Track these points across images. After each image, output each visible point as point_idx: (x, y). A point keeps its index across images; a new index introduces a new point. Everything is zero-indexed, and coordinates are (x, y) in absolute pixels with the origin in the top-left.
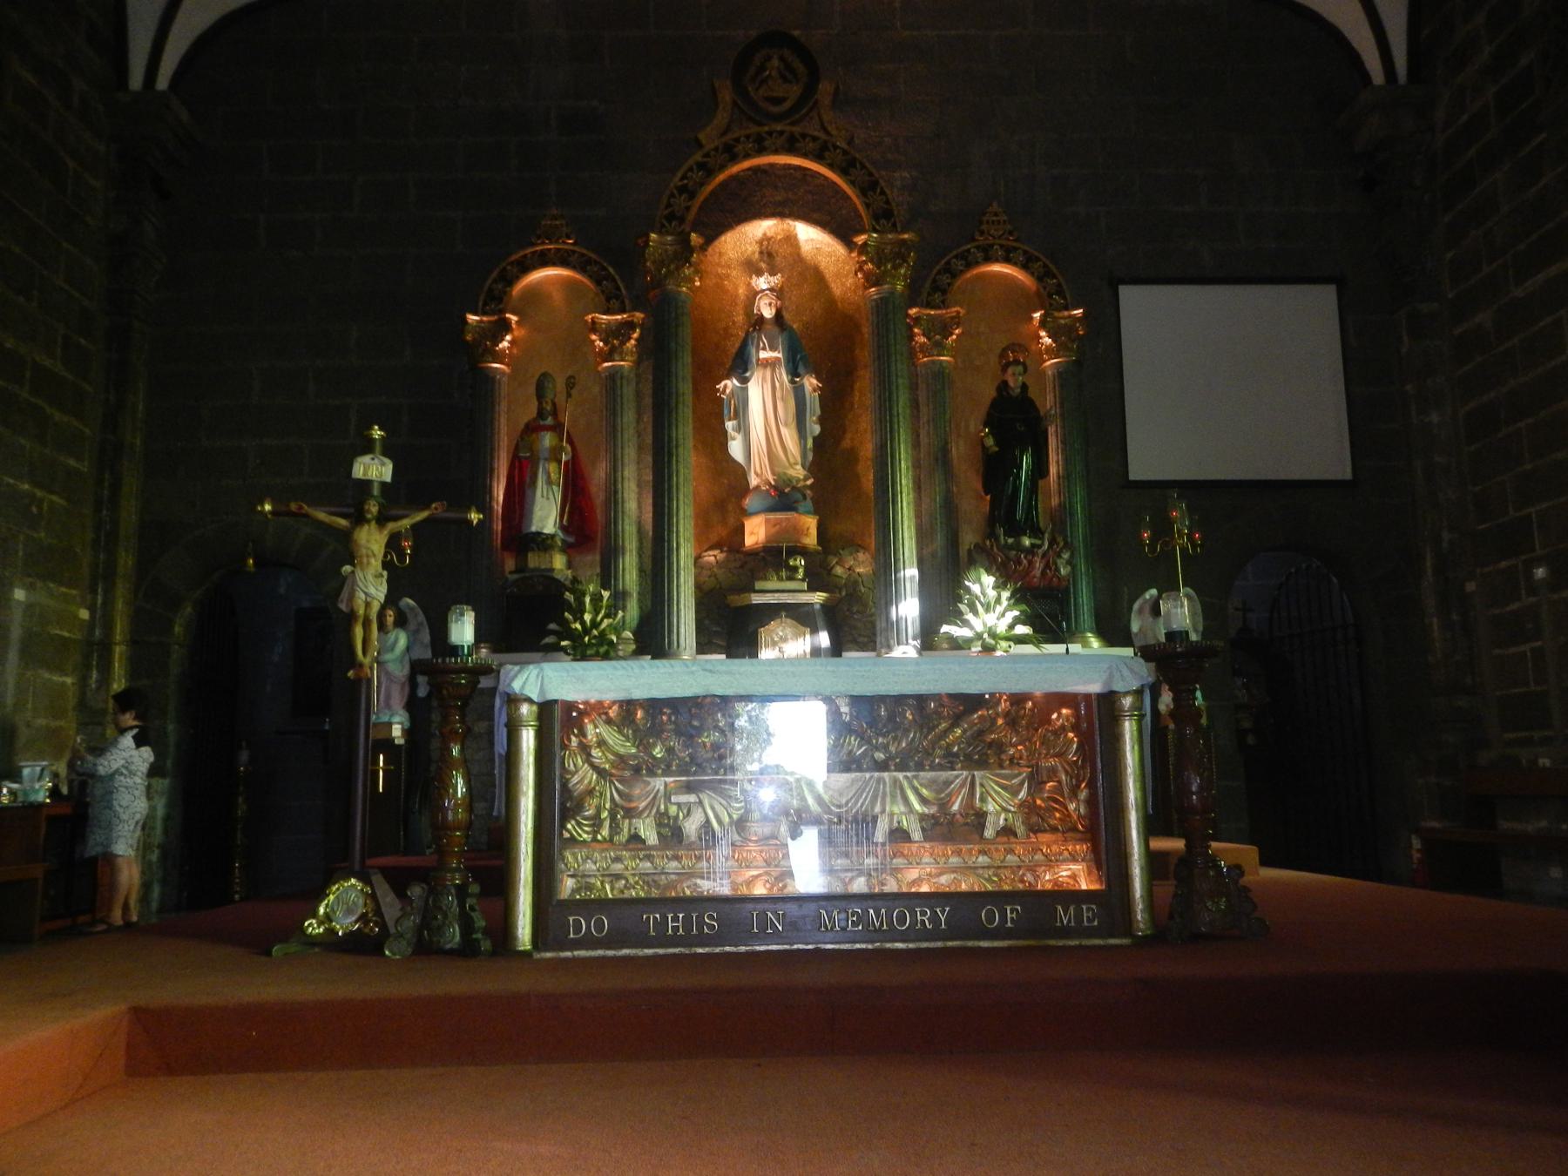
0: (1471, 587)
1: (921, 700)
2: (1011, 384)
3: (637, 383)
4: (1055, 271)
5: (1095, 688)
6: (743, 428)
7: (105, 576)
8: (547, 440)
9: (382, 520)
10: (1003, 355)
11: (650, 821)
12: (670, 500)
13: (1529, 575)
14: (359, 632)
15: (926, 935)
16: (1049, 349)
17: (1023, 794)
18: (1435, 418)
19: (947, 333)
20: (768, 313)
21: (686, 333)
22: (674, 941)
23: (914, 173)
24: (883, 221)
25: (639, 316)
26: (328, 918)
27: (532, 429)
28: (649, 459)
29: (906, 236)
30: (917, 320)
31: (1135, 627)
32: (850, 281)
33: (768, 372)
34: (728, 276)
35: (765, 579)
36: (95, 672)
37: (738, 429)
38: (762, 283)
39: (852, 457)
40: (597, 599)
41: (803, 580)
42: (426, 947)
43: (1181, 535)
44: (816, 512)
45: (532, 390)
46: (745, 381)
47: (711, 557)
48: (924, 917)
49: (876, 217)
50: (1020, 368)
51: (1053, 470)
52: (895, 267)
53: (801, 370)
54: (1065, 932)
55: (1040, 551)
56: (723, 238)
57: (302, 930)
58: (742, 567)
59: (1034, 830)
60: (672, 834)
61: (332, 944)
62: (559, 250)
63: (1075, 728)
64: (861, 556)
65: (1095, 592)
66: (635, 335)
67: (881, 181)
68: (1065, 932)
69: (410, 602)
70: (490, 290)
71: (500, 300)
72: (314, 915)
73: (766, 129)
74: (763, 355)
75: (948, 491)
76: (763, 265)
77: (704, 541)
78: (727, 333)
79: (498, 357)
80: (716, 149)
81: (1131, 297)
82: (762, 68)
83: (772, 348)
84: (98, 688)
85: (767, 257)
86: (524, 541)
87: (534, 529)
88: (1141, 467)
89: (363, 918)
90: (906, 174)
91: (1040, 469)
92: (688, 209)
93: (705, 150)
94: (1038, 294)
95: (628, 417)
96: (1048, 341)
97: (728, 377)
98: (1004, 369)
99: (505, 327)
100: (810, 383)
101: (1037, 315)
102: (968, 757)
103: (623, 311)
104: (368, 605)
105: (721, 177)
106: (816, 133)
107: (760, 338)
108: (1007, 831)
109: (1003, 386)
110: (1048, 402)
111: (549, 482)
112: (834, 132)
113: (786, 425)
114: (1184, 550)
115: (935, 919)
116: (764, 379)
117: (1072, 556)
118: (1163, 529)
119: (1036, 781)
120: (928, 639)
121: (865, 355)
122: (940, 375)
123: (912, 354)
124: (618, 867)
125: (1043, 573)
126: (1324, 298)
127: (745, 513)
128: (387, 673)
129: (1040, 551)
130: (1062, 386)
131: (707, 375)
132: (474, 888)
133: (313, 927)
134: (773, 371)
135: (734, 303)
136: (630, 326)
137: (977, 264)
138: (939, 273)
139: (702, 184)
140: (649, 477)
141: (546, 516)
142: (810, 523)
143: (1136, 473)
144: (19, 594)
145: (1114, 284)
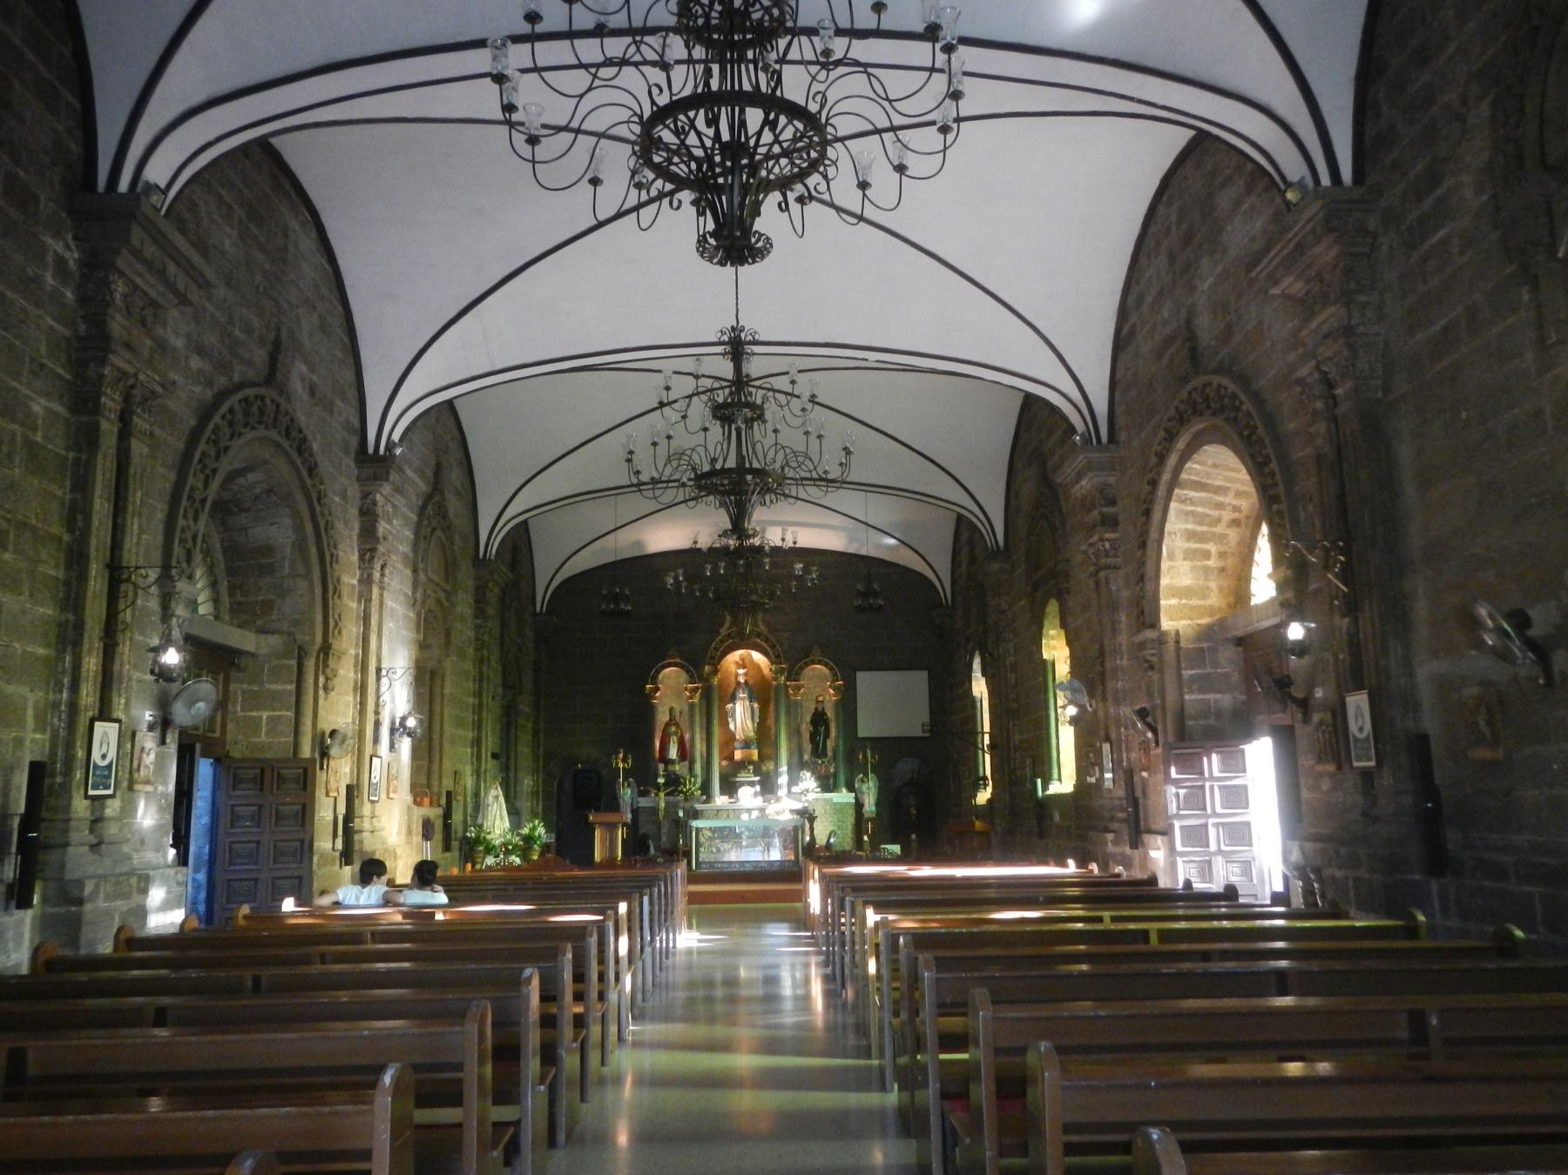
7: (536, 771)
8: (673, 729)
20: (742, 681)
21: (716, 697)
27: (668, 725)
28: (705, 731)
30: (789, 686)
31: (856, 786)
38: (741, 671)
40: (690, 781)
45: (667, 709)
46: (735, 704)
47: (724, 763)
51: (833, 733)
60: (719, 850)
77: (722, 758)
78: (729, 686)
81: (860, 675)
88: (861, 733)
91: (827, 735)
95: (697, 718)
99: (657, 689)
100: (756, 705)
110: (830, 713)
118: (865, 756)
119: (785, 841)
120: (789, 792)
121: (772, 694)
122: (797, 704)
123: (787, 695)
126: (924, 675)
131: (723, 703)
136: (698, 688)
140: (705, 736)
141: (673, 753)
142: (755, 754)
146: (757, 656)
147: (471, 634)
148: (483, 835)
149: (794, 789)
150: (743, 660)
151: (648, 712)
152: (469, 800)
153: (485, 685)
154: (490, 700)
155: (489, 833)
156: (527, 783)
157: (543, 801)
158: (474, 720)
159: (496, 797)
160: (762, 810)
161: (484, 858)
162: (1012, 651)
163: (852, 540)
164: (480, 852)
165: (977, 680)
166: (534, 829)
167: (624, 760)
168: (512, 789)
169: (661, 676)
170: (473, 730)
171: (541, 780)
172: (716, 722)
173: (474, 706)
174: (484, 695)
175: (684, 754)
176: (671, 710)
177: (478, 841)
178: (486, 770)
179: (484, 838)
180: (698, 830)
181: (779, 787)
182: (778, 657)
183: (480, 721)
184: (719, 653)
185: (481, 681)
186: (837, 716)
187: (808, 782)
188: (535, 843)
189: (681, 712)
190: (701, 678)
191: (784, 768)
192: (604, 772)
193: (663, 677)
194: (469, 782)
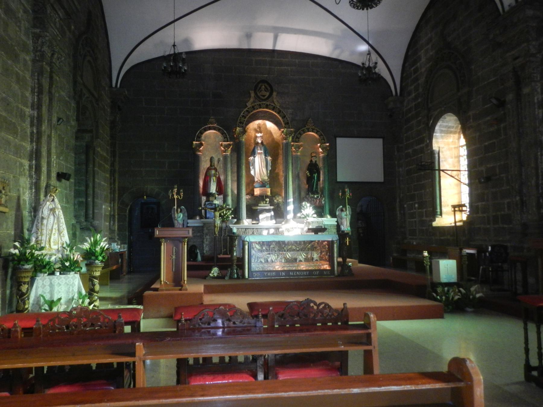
0: (405, 206)
1: (304, 242)
2: (313, 160)
3: (231, 158)
4: (323, 134)
5: (330, 240)
6: (254, 168)
7: (112, 200)
8: (213, 172)
9: (219, 211)
10: (311, 154)
11: (263, 259)
12: (241, 187)
13: (415, 206)
14: (216, 229)
15: (305, 276)
16: (321, 152)
17: (319, 255)
18: (401, 169)
19: (299, 147)
20: (260, 141)
21: (244, 149)
22: (269, 276)
23: (293, 110)
24: (287, 125)
25: (232, 142)
26: (213, 274)
27: (209, 169)
29: (292, 130)
30: (293, 145)
31: (337, 214)
32: (278, 135)
33: (260, 156)
34: (250, 132)
35: (260, 203)
36: (112, 222)
37: (253, 168)
38: (259, 135)
39: (278, 175)
41: (269, 204)
42: (231, 278)
43: (347, 195)
44: (270, 187)
45: (208, 158)
46: (255, 157)
47: (248, 197)
48: (305, 273)
49: (285, 124)
50: (315, 157)
51: (321, 179)
52: (289, 136)
53: (267, 155)
54: (325, 275)
55: (318, 199)
56: (250, 124)
57: (210, 276)
58: (254, 200)
59: (321, 260)
60: (267, 261)
61: (214, 278)
62: (213, 126)
63: (327, 245)
64: (280, 197)
65: (329, 205)
66: (231, 147)
67: (287, 116)
68: (325, 275)
69: (183, 207)
70: (198, 135)
71: (200, 138)
72: (211, 273)
73: (262, 103)
74: (259, 151)
75: (299, 183)
76: (258, 130)
78: (250, 145)
79: (200, 151)
80: (250, 107)
81: (339, 141)
82: (260, 88)
83: (261, 150)
84: (113, 225)
85: (259, 129)
86: (209, 195)
87: (211, 192)
89: (218, 274)
90: (291, 111)
92: (244, 121)
93: (248, 107)
94: (319, 139)
95: (229, 166)
96: (320, 150)
97: (251, 156)
98: (312, 157)
99: (201, 145)
100: (269, 158)
101: (319, 145)
102: (311, 249)
103: (228, 141)
104: (217, 225)
105: (252, 113)
106: (272, 104)
107: (258, 148)
108: (317, 260)
109: (311, 161)
110: (321, 165)
111: (214, 181)
112: (276, 104)
113: (264, 167)
114: (348, 198)
115: (307, 273)
116: (259, 157)
117: (325, 199)
118: (344, 193)
119: (321, 253)
120: (295, 217)
121: (281, 152)
123: (292, 152)
124: (258, 266)
125: (319, 203)
126: (380, 141)
127: (254, 187)
128: (179, 223)
129: (318, 199)
130: (324, 160)
132: (238, 269)
133: (211, 275)
134: (261, 155)
135: (252, 138)
136: (230, 145)
137: (306, 132)
138: (298, 134)
139: (247, 115)
141: (213, 189)
142: (269, 190)
143: (338, 180)
144: (104, 207)
145: (336, 137)
146: (270, 125)
147: (30, 42)
148: (28, 251)
149: (299, 215)
150: (259, 127)
151: (195, 161)
152: (26, 213)
153: (46, 99)
154: (55, 119)
155: (42, 249)
156: (105, 208)
157: (118, 221)
158: (32, 133)
159: (53, 210)
160: (277, 229)
161: (33, 279)
162: (539, 90)
163: (336, 47)
164: (26, 271)
165: (437, 138)
166: (96, 243)
167: (178, 193)
168: (91, 212)
169: (203, 136)
170: (32, 142)
171: (116, 207)
172: (244, 167)
173: (32, 118)
174: (44, 109)
175: (221, 190)
176: (211, 159)
177: (23, 258)
178: (48, 186)
179: (32, 255)
180: (250, 244)
181: (288, 212)
182: (287, 123)
183: (39, 134)
184: (246, 119)
185: (40, 92)
186: (324, 167)
187: (308, 210)
188: (97, 258)
189: (219, 161)
190: (232, 139)
191: (291, 200)
192: (163, 202)
193: (205, 137)
194: (27, 197)
